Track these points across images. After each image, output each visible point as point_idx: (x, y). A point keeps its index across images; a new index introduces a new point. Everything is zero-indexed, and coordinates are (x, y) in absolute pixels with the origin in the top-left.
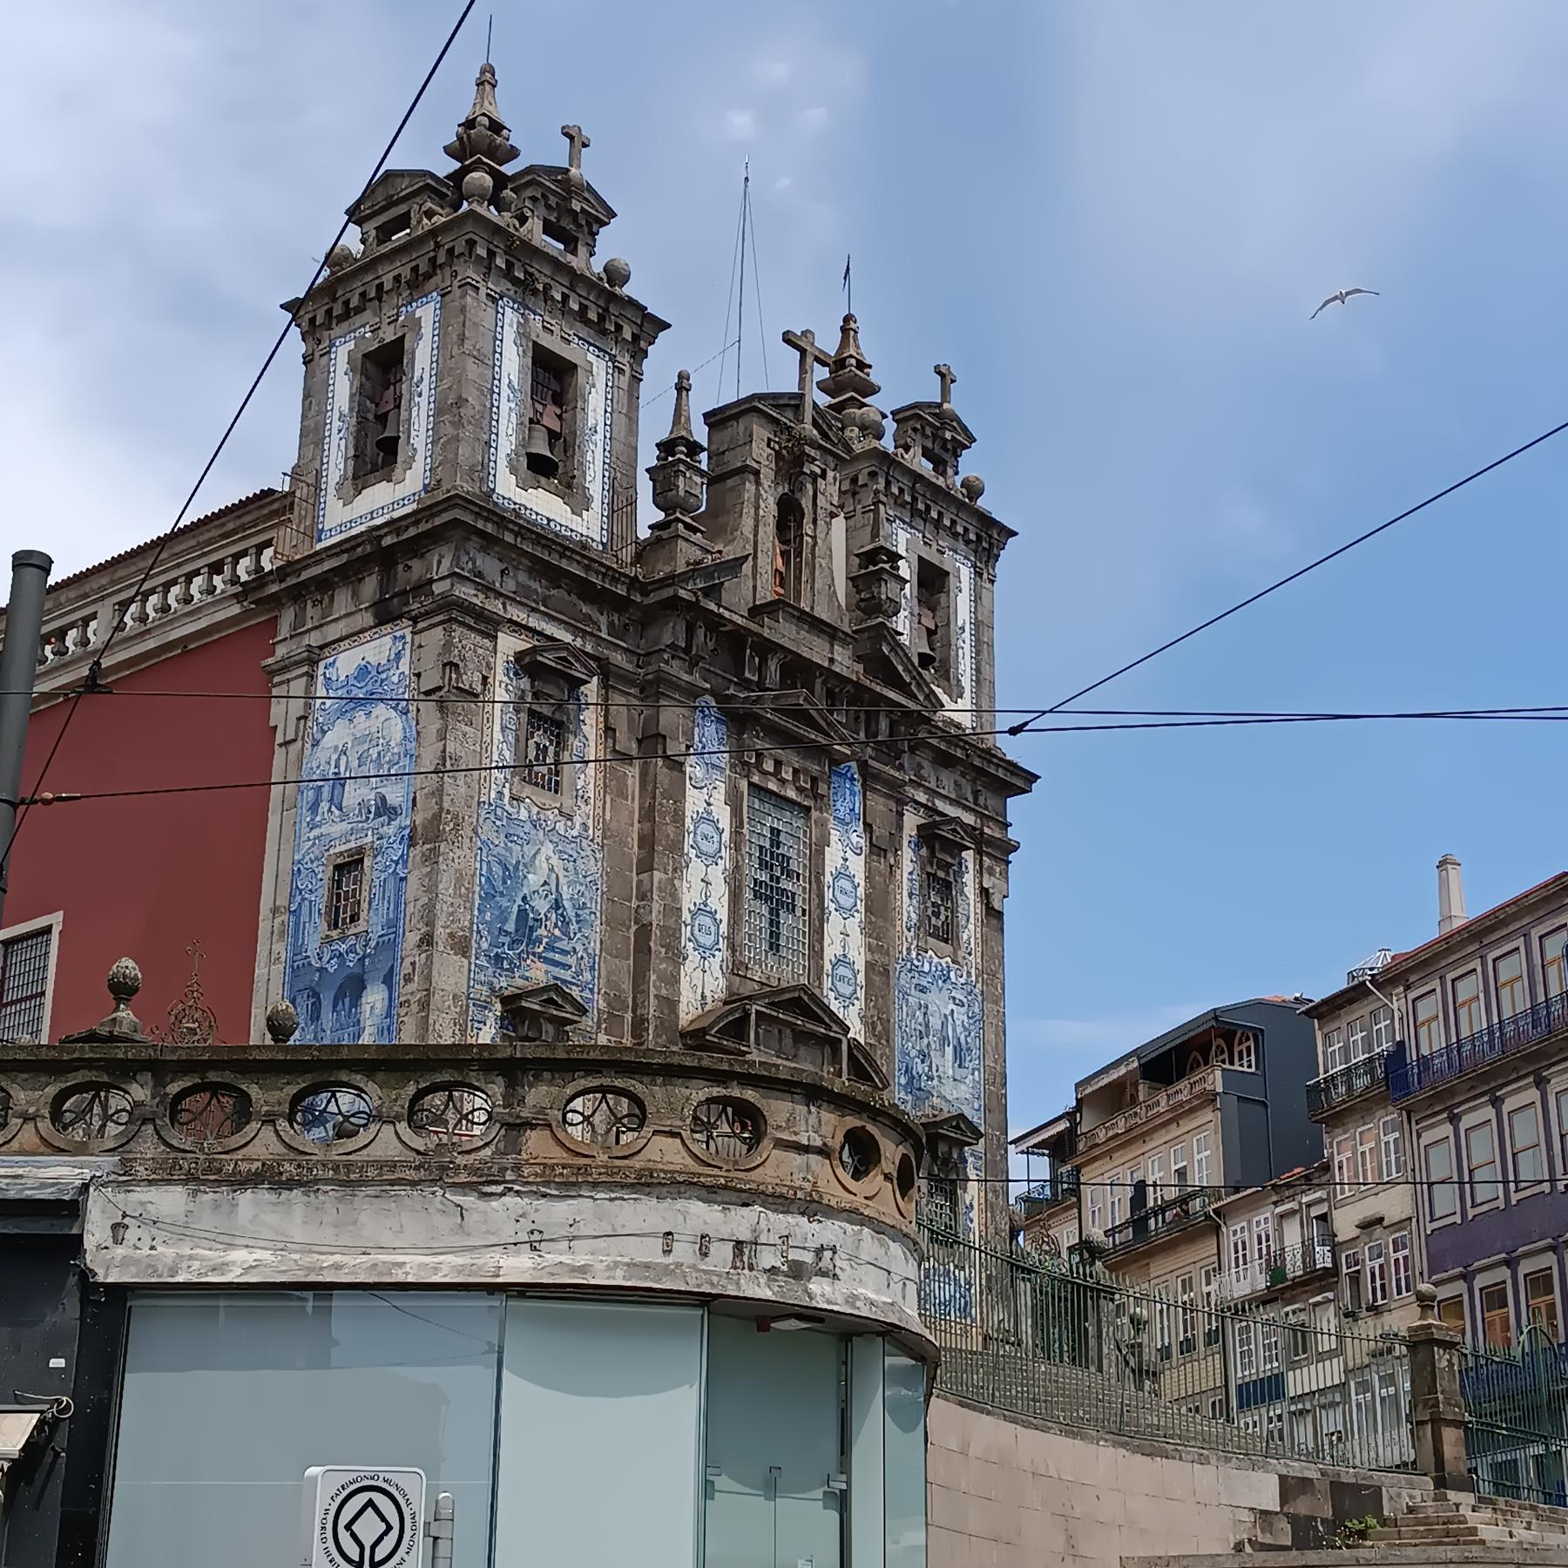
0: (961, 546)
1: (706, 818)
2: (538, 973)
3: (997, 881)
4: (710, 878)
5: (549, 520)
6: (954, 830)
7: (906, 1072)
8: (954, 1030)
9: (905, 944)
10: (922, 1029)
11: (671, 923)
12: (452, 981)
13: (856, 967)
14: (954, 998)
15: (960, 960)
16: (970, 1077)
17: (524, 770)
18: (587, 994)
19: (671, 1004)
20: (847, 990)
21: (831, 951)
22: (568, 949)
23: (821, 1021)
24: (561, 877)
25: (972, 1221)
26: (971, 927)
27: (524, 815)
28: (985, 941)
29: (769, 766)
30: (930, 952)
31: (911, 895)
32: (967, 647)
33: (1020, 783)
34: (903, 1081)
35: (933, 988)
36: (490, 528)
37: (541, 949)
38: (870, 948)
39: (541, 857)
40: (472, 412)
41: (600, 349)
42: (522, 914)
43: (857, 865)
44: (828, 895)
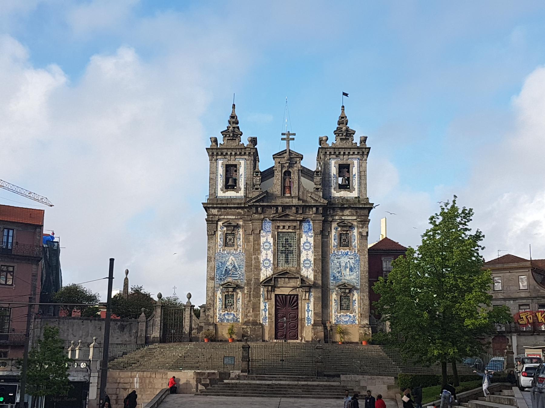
0: (354, 156)
1: (267, 242)
2: (229, 279)
3: (363, 229)
4: (268, 253)
5: (231, 197)
6: (345, 223)
7: (333, 276)
8: (350, 265)
9: (333, 250)
10: (339, 267)
11: (258, 264)
12: (211, 285)
13: (311, 260)
14: (349, 258)
15: (352, 249)
16: (355, 273)
17: (226, 244)
18: (242, 280)
20: (308, 265)
21: (302, 259)
22: (237, 273)
24: (235, 262)
25: (355, 303)
26: (356, 241)
27: (226, 252)
28: (361, 243)
29: (282, 228)
30: (342, 250)
31: (335, 240)
32: (356, 179)
34: (332, 278)
35: (343, 257)
36: (210, 206)
37: (230, 275)
38: (315, 255)
39: (230, 259)
41: (242, 159)
42: (226, 270)
43: (311, 240)
44: (302, 248)
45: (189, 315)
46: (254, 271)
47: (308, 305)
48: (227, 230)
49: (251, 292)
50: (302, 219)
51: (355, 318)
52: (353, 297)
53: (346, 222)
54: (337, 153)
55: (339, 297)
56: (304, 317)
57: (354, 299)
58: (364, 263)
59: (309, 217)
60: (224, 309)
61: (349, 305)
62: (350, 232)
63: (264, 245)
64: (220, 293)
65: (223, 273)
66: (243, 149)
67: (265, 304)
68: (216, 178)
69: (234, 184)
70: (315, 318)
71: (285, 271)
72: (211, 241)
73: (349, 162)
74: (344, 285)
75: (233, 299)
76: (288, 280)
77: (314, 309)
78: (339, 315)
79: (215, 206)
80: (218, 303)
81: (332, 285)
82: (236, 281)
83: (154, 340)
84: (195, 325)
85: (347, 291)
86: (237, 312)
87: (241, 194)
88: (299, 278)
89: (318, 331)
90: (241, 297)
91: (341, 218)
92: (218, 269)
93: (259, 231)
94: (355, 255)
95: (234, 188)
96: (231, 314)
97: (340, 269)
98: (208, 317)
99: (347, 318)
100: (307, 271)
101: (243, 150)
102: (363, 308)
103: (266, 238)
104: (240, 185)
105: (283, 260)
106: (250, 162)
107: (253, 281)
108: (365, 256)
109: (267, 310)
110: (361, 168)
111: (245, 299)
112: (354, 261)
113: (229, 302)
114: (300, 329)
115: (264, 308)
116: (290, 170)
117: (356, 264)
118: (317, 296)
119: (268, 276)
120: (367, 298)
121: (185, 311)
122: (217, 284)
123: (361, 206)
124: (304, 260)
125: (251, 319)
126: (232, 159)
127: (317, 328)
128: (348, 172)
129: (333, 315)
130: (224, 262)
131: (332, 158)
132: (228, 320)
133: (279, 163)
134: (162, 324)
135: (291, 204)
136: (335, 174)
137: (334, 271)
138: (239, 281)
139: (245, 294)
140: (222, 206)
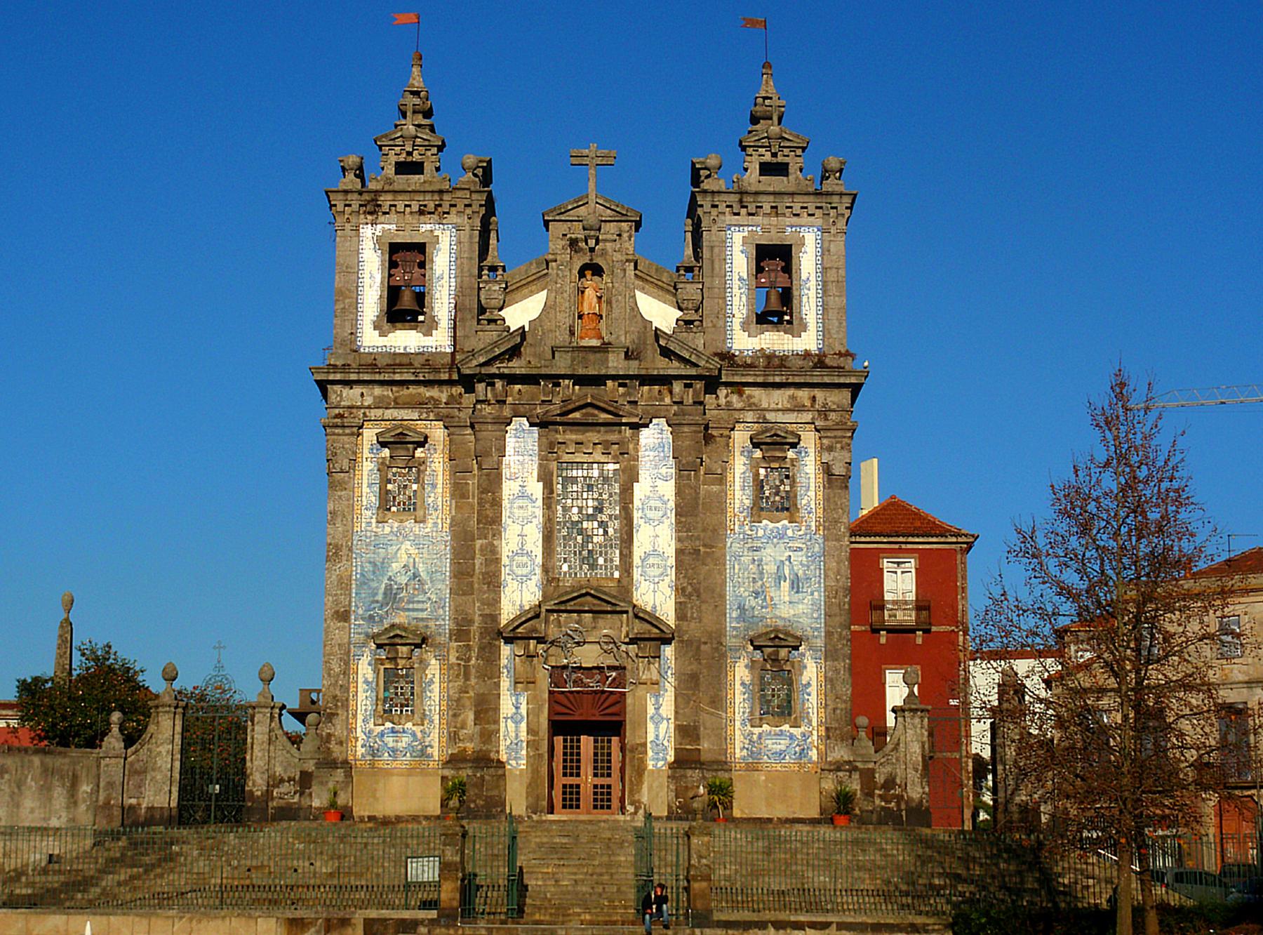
0: (805, 219)
2: (400, 618)
3: (836, 454)
4: (525, 532)
7: (739, 608)
8: (792, 569)
11: (492, 568)
13: (666, 555)
17: (385, 503)
19: (494, 618)
23: (608, 602)
24: (417, 560)
25: (809, 695)
26: (812, 494)
28: (827, 499)
30: (765, 522)
32: (812, 293)
33: (853, 380)
34: (734, 615)
36: (338, 377)
38: (679, 540)
40: (342, 306)
42: (389, 589)
43: (668, 489)
44: (636, 515)
45: (267, 736)
46: (480, 590)
47: (657, 702)
48: (391, 457)
49: (469, 659)
50: (636, 420)
51: (810, 740)
52: (801, 674)
53: (779, 432)
54: (752, 208)
55: (757, 672)
56: (643, 741)
57: (804, 681)
58: (838, 563)
59: (662, 415)
60: (381, 717)
61: (789, 702)
62: (793, 465)
63: (515, 505)
64: (369, 664)
65: (380, 597)
66: (447, 191)
67: (517, 700)
68: (358, 287)
69: (417, 309)
70: (681, 744)
71: (584, 591)
72: (339, 493)
73: (788, 236)
74: (772, 636)
75: (412, 682)
76: (594, 618)
77: (676, 712)
78: (757, 731)
79: (353, 377)
80: (361, 696)
81: (735, 637)
82: (421, 624)
83: (152, 816)
84: (285, 771)
85: (783, 653)
86: (423, 725)
87: (440, 340)
88: (627, 612)
89: (690, 785)
90: (437, 676)
91: (764, 418)
92: (364, 582)
93: (496, 458)
94: (808, 537)
95: (415, 320)
96: (404, 732)
97: (760, 582)
98: (329, 743)
99: (782, 742)
100: (654, 592)
101: (446, 197)
102: (834, 710)
103: (519, 482)
104: (436, 309)
105: (575, 555)
106: (471, 237)
107: (476, 624)
108: (838, 540)
109: (522, 717)
110: (825, 257)
111: (450, 681)
112: (804, 559)
113: (396, 694)
114: (631, 780)
115: (514, 710)
116: (599, 261)
117: (812, 567)
118: (688, 670)
119: (527, 608)
120: (844, 675)
121: (252, 721)
122: (359, 634)
123: (826, 380)
124: (643, 555)
125: (470, 746)
126: (408, 228)
127: (686, 777)
128: (788, 269)
129: (738, 732)
130: (383, 563)
131: (735, 225)
132: (394, 750)
133: (565, 235)
134: (177, 764)
135: (603, 372)
136: (745, 277)
137: (742, 589)
138: (431, 624)
139: (450, 667)
140: (377, 377)
